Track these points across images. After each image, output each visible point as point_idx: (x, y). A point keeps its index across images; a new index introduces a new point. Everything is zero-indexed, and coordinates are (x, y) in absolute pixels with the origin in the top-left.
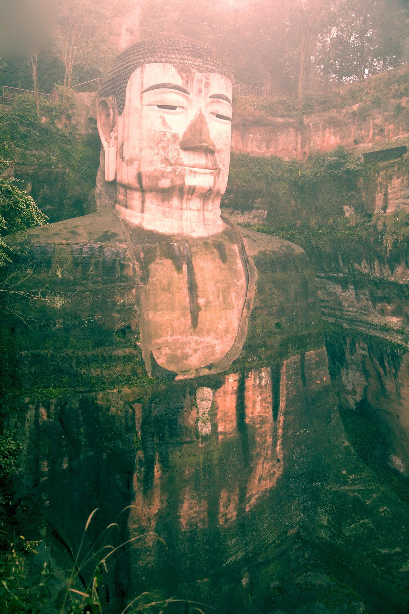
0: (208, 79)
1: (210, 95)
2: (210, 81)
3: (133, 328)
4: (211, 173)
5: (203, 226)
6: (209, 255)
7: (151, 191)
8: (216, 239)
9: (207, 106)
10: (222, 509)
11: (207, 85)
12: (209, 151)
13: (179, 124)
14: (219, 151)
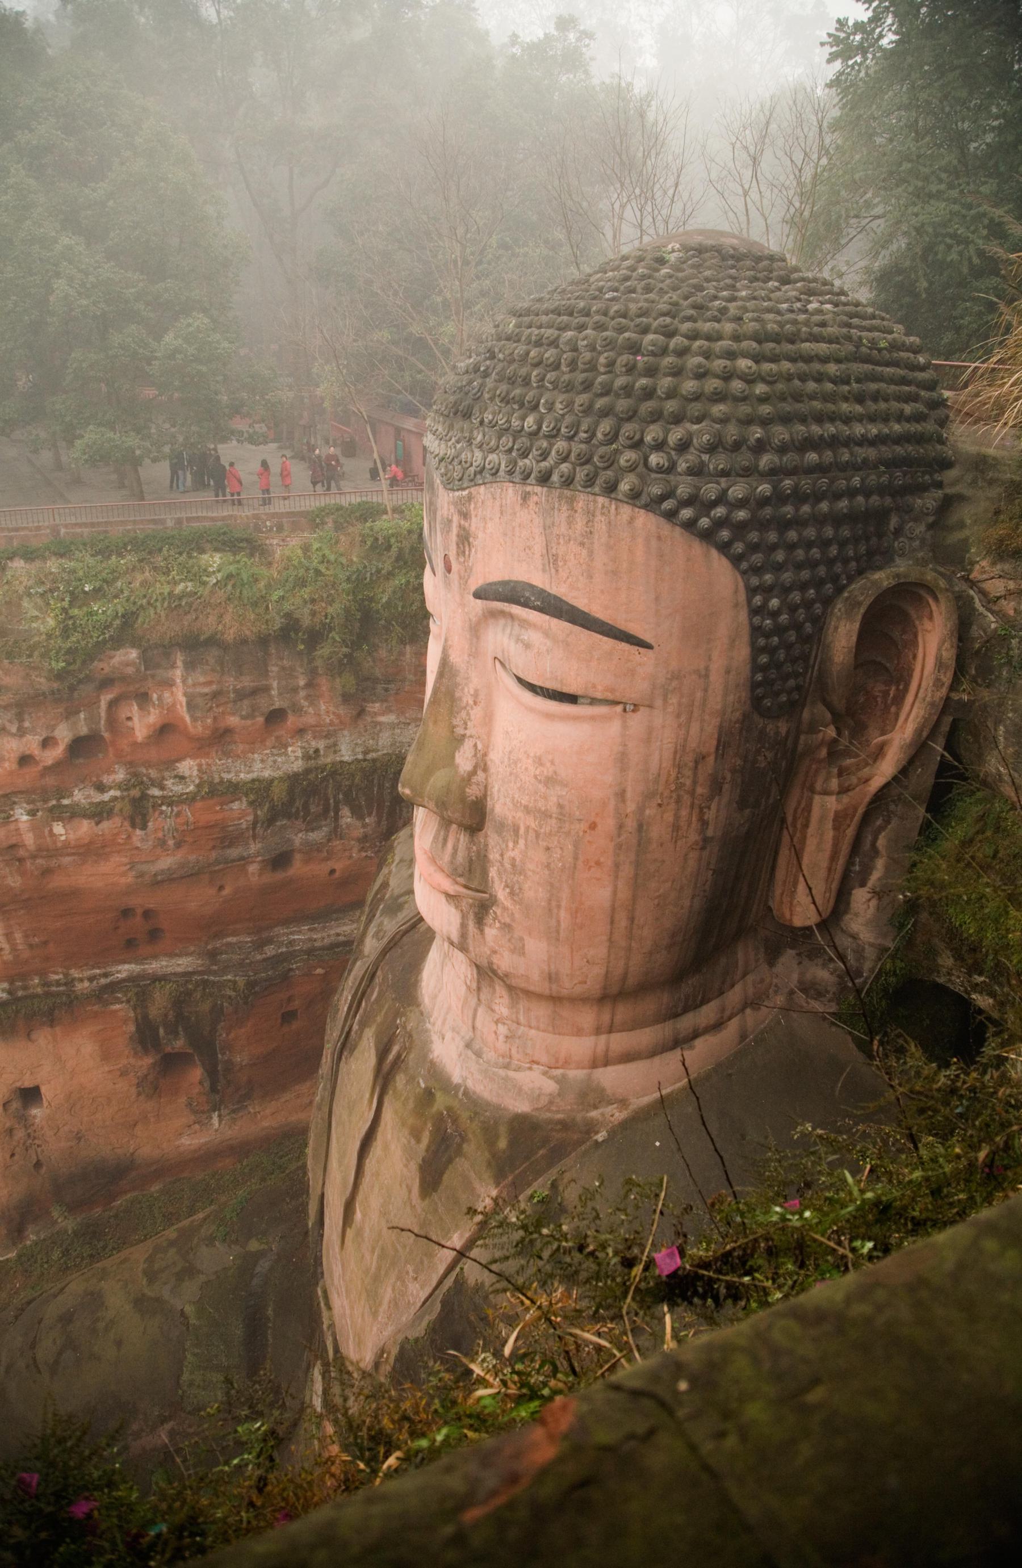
0: (465, 516)
1: (473, 588)
2: (474, 524)
4: (448, 896)
5: (462, 1044)
6: (406, 1132)
8: (464, 1115)
9: (475, 630)
11: (465, 539)
14: (501, 827)
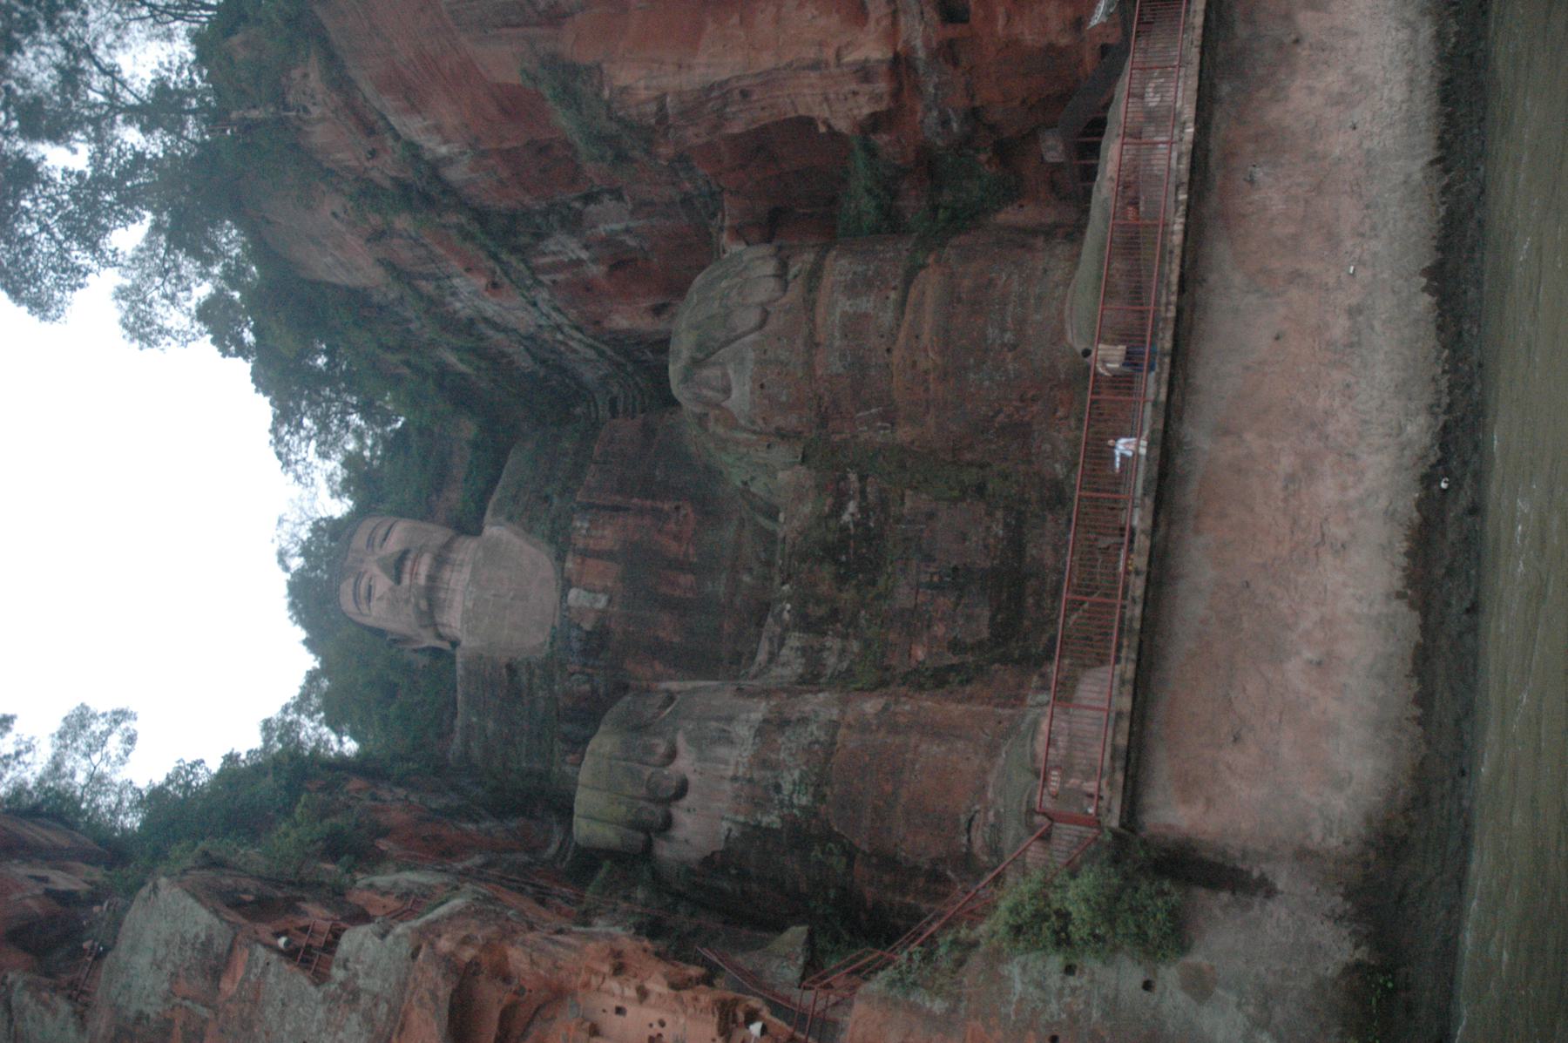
3: (505, 660)
7: (432, 617)
10: (678, 593)
12: (402, 557)
13: (383, 584)
